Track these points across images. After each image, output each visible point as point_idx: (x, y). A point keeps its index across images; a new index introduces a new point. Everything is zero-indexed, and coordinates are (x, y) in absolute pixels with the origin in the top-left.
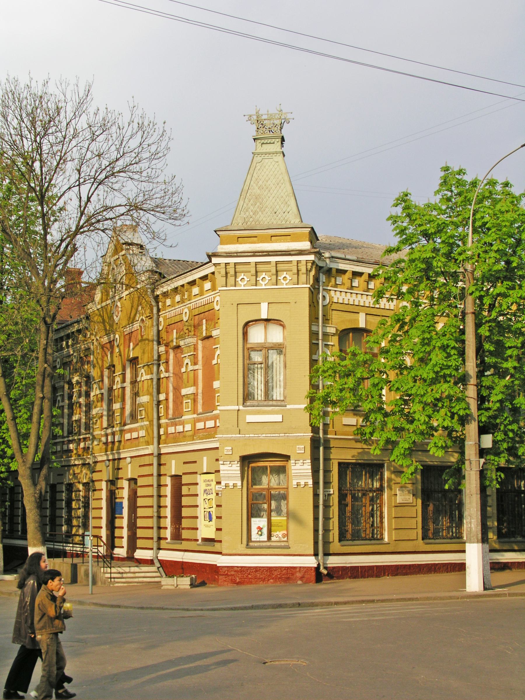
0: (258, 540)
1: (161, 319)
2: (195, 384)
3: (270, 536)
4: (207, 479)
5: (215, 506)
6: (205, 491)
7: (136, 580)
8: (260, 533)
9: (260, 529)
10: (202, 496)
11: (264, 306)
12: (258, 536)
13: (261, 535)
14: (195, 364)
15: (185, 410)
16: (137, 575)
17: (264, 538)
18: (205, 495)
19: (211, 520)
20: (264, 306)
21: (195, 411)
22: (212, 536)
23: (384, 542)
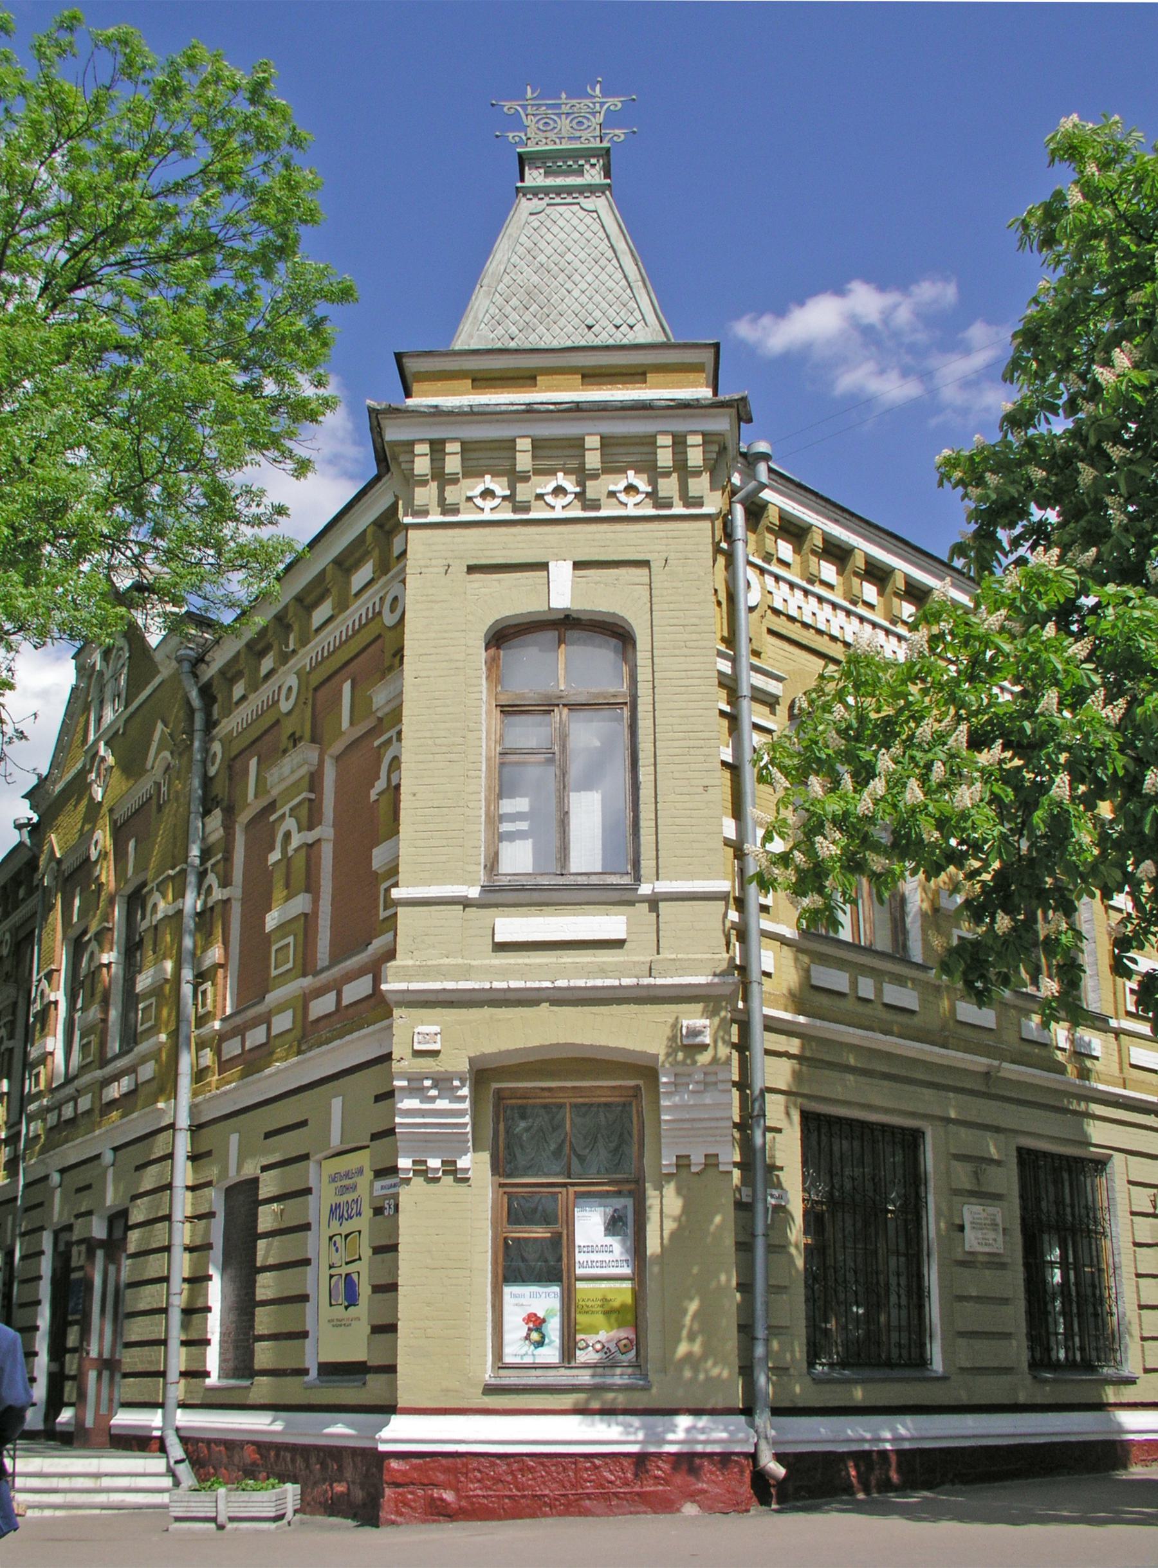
0: (528, 1360)
1: (216, 747)
2: (311, 887)
3: (569, 1350)
4: (342, 1171)
5: (366, 1252)
6: (334, 1210)
7: (101, 1498)
8: (535, 1336)
9: (536, 1323)
10: (324, 1228)
11: (561, 572)
12: (528, 1348)
13: (540, 1344)
14: (312, 823)
15: (274, 973)
16: (106, 1482)
17: (550, 1353)
18: (335, 1223)
19: (352, 1299)
20: (561, 572)
21: (306, 967)
22: (358, 1353)
23: (928, 1374)
